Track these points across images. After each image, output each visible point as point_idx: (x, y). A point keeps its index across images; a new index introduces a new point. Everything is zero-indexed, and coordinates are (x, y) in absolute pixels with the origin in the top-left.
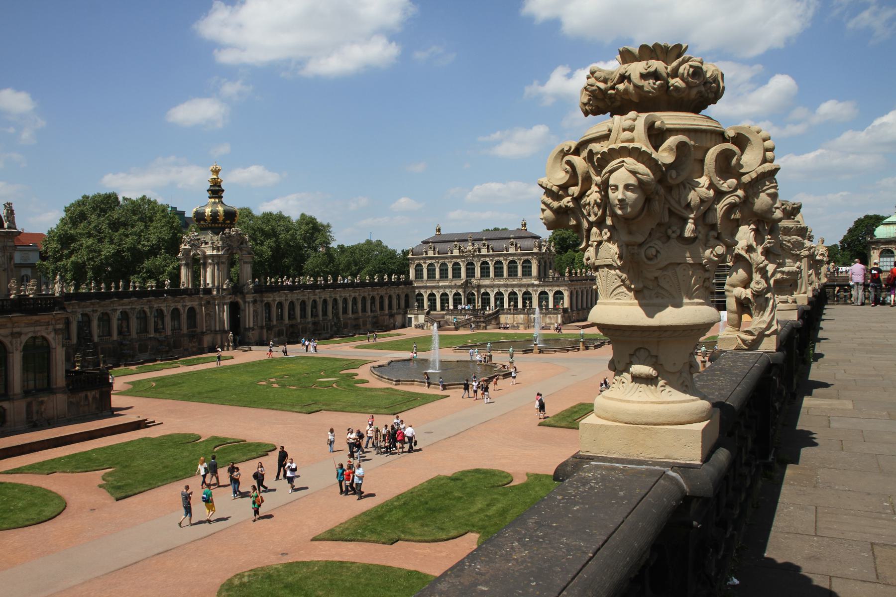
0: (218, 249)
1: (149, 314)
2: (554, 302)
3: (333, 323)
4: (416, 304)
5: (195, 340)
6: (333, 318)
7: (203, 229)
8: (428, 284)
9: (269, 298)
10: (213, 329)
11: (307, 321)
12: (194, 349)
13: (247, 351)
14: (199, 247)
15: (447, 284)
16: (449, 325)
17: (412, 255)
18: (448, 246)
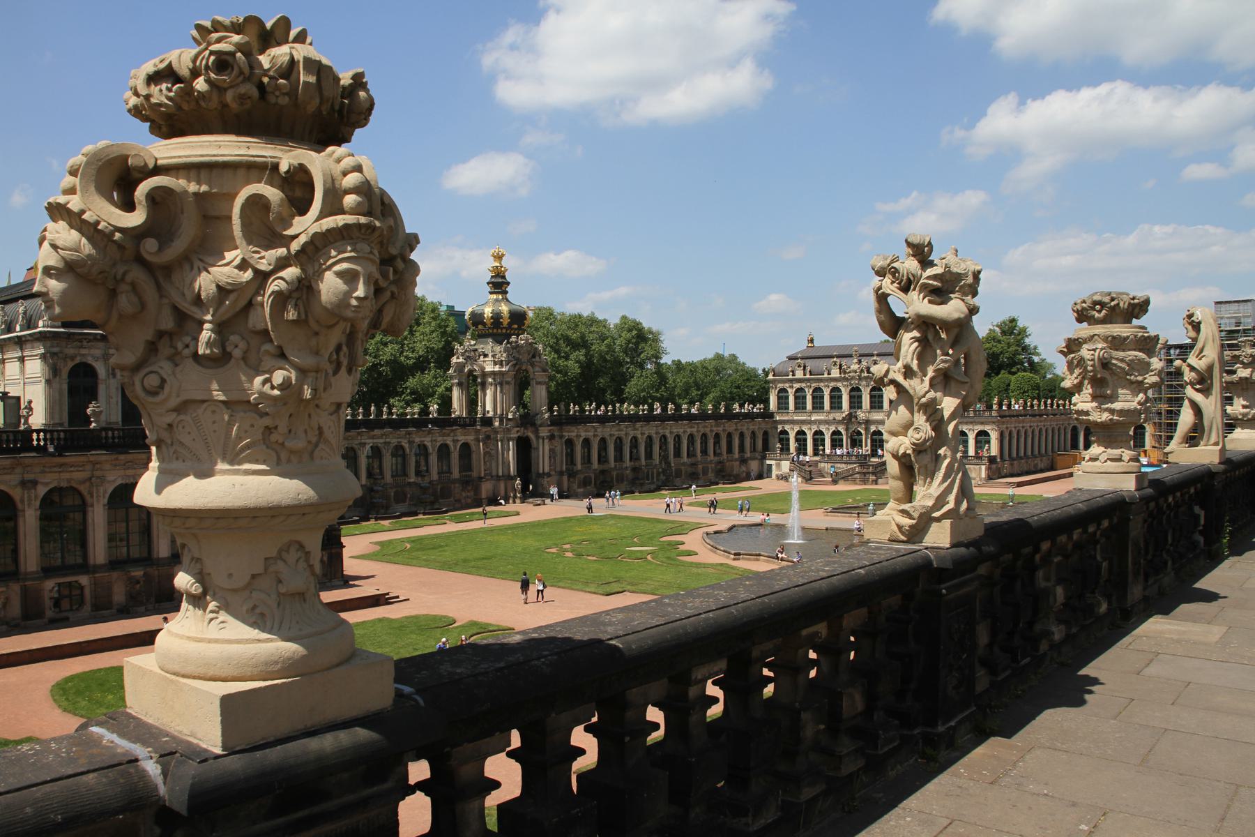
0: (501, 363)
1: (408, 450)
2: (977, 448)
3: (660, 470)
4: (778, 445)
5: (470, 488)
6: (660, 463)
7: (480, 336)
8: (795, 418)
9: (571, 432)
10: (494, 473)
11: (624, 466)
12: (469, 501)
13: (539, 505)
14: (476, 361)
15: (822, 418)
16: (824, 477)
17: (774, 375)
18: (823, 364)
